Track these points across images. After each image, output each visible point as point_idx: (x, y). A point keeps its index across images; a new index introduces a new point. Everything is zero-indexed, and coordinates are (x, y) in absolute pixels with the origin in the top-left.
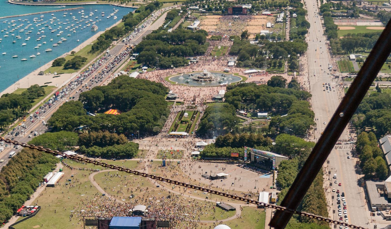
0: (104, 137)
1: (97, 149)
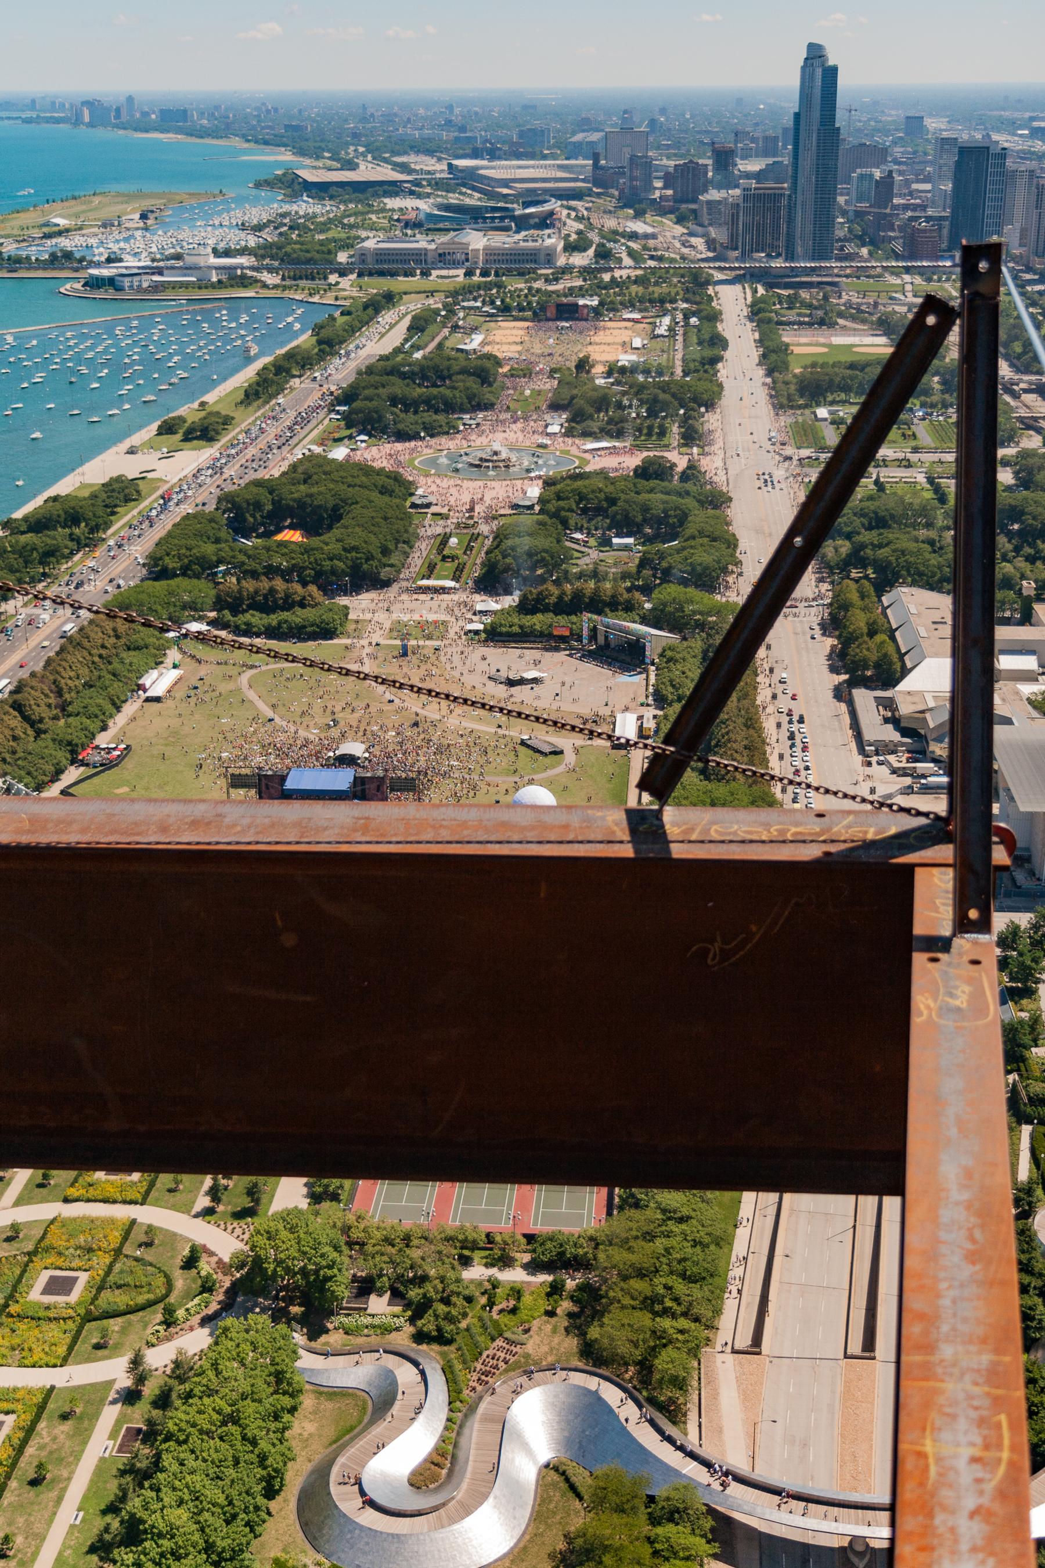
0: (272, 591)
1: (255, 618)
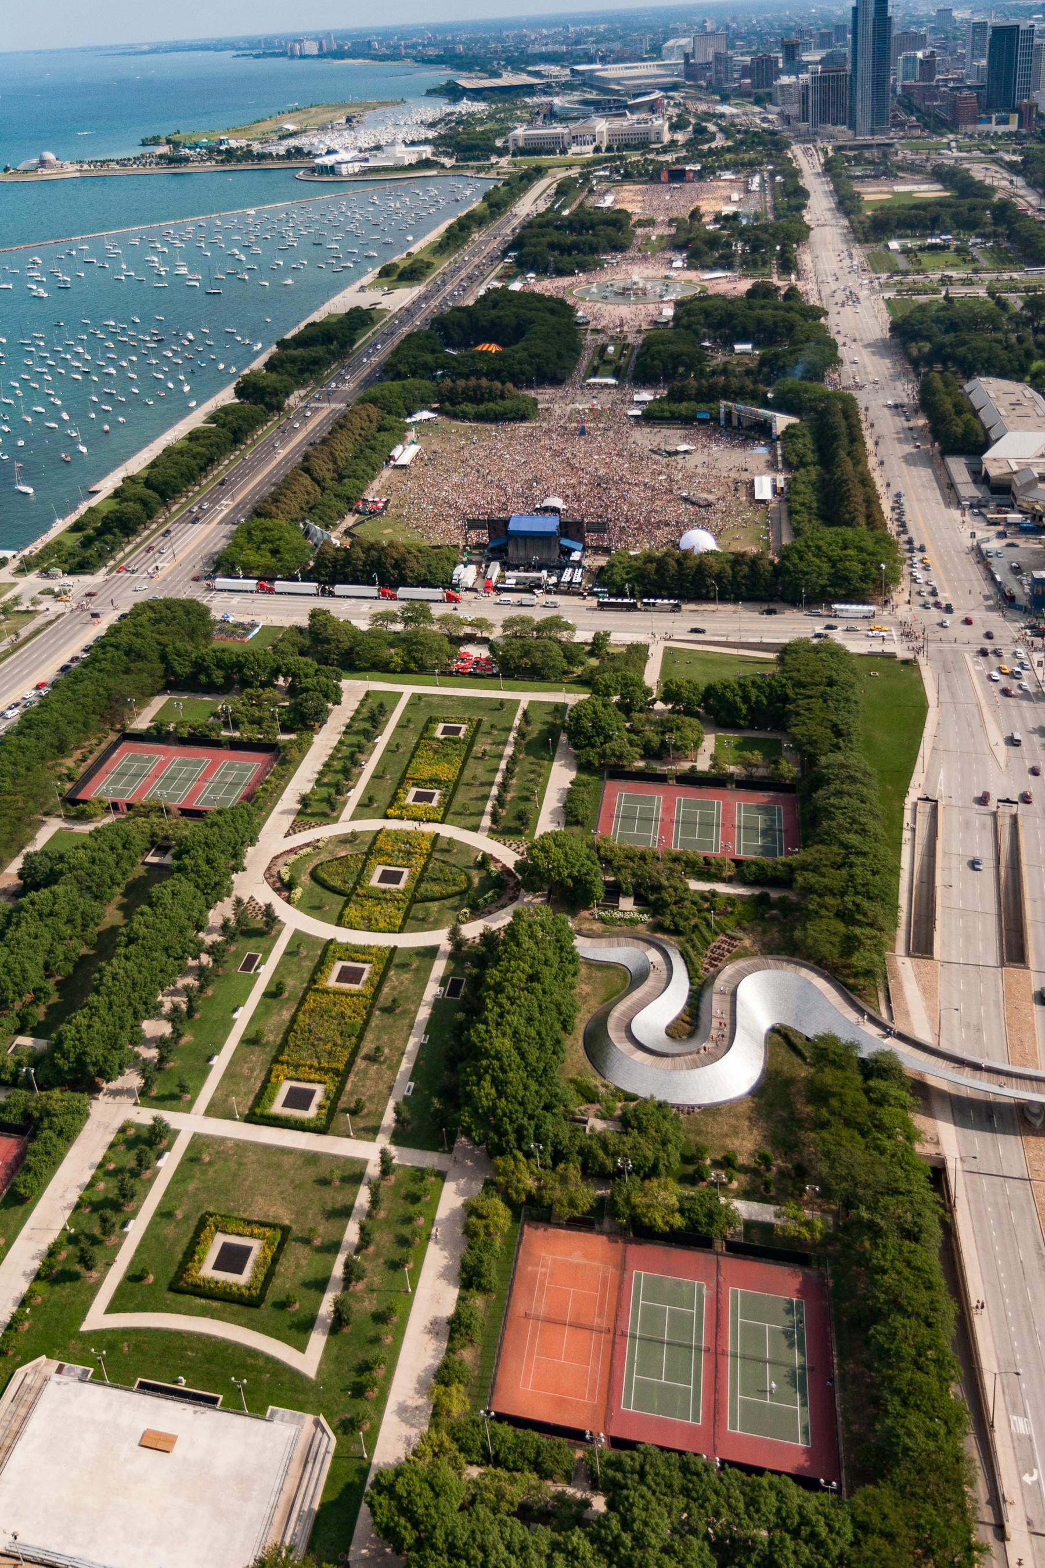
0: (479, 387)
1: (469, 408)
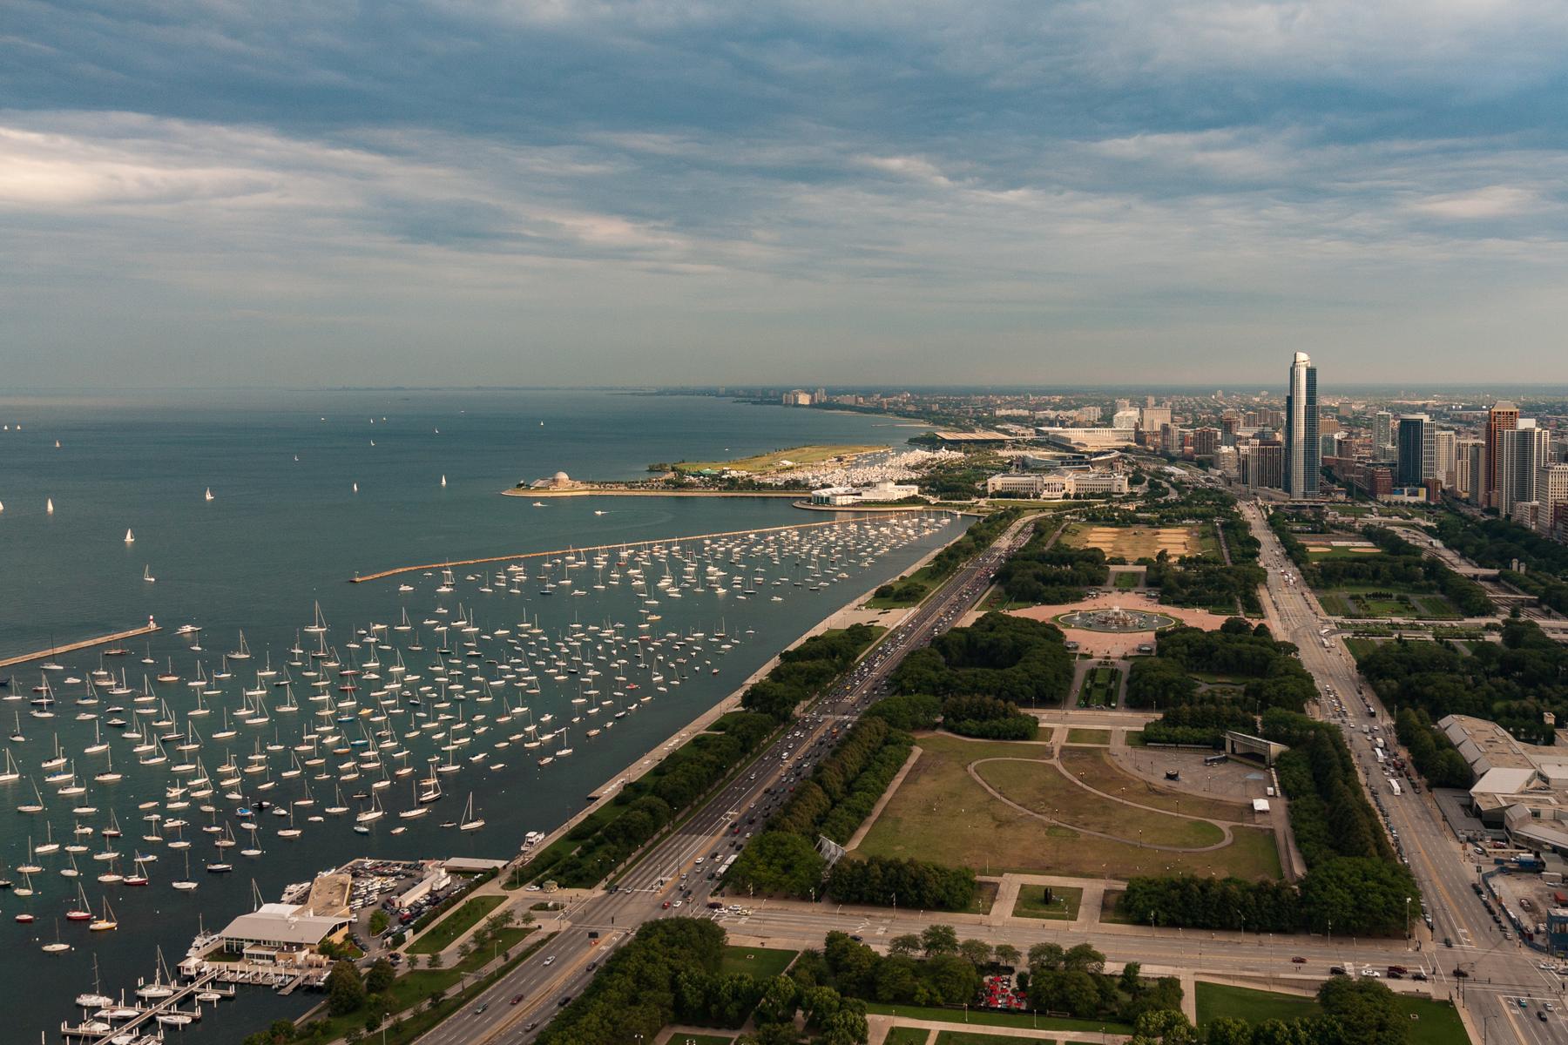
1: (970, 723)
